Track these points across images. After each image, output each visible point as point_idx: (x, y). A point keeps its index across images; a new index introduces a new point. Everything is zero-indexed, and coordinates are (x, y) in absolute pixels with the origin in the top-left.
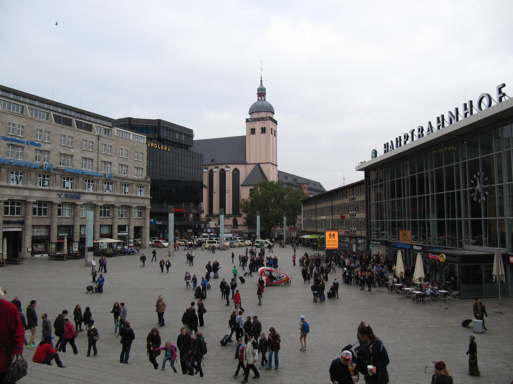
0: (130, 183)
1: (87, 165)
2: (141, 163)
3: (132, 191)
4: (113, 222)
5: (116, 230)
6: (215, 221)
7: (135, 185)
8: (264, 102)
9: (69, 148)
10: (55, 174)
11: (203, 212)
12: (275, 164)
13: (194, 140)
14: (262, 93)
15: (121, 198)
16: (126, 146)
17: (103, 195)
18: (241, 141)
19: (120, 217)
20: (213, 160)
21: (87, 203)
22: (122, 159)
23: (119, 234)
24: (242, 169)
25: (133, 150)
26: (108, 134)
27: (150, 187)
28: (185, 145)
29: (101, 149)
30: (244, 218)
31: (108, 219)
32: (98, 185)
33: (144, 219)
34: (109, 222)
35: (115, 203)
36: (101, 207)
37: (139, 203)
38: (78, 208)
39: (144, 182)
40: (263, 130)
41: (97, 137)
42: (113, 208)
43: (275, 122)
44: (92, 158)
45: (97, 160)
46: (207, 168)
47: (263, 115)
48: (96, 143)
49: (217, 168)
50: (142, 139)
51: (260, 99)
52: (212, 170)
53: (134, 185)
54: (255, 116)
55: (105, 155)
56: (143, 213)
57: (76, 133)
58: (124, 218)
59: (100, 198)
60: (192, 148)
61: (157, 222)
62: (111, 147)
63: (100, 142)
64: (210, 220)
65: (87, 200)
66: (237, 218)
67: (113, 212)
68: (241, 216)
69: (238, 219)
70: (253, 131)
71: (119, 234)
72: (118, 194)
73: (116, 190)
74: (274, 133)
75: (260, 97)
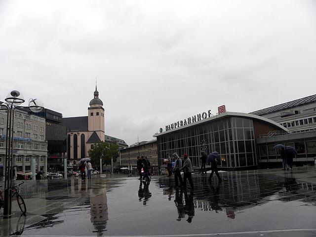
14: (96, 94)
18: (85, 119)
24: (86, 134)
40: (98, 114)
47: (97, 106)
48: (23, 124)
50: (42, 121)
54: (93, 106)
70: (92, 114)
74: (103, 115)
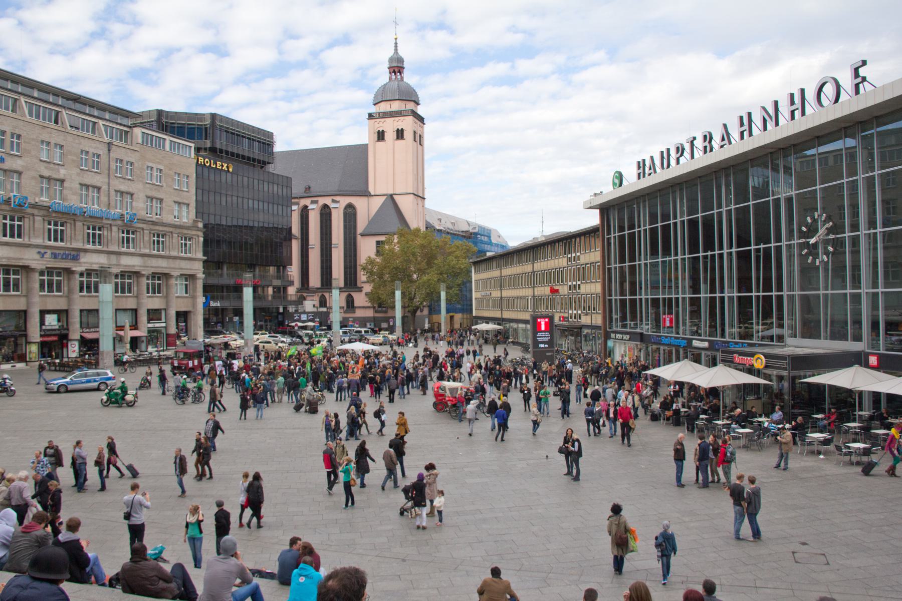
1: (90, 197)
2: (185, 194)
3: (171, 247)
8: (401, 83)
9: (57, 167)
10: (33, 215)
12: (421, 196)
13: (274, 151)
16: (159, 163)
19: (150, 295)
20: (308, 189)
22: (151, 186)
24: (359, 203)
25: (170, 170)
26: (126, 141)
28: (259, 161)
29: (115, 168)
35: (142, 268)
38: (75, 278)
41: (106, 145)
43: (421, 119)
44: (99, 184)
45: (107, 189)
46: (298, 204)
49: (316, 202)
51: (394, 77)
52: (306, 207)
54: (384, 107)
55: (121, 180)
57: (70, 138)
60: (272, 166)
62: (132, 164)
63: (112, 155)
70: (381, 136)
73: (142, 244)
74: (419, 139)
75: (393, 74)
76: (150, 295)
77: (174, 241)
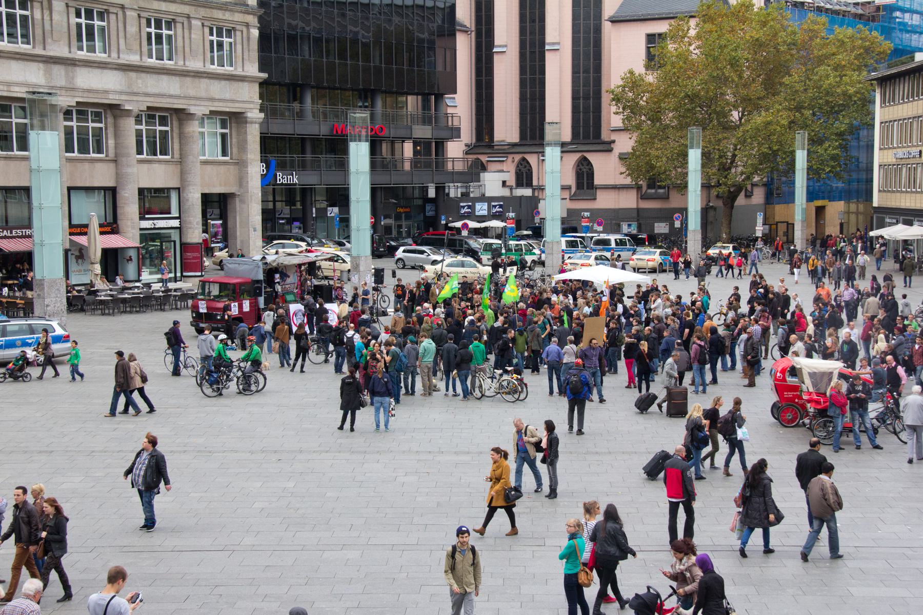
0: (176, 14)
3: (187, 49)
4: (118, 176)
5: (130, 207)
6: (502, 171)
7: (199, 23)
11: (455, 133)
15: (143, 75)
17: (71, 63)
19: (144, 156)
21: (30, 96)
23: (146, 224)
27: (255, 33)
30: (623, 157)
31: (99, 165)
32: (47, 18)
33: (241, 164)
34: (102, 176)
35: (124, 97)
36: (68, 114)
37: (220, 100)
39: (231, 11)
42: (115, 117)
53: (194, 22)
56: (234, 140)
58: (160, 161)
59: (59, 75)
61: (279, 175)
64: (484, 168)
65: (28, 85)
66: (594, 158)
67: (116, 136)
68: (607, 147)
69: (597, 160)
71: (146, 224)
72: (134, 59)
73: (122, 41)
76: (144, 156)
77: (193, 36)
